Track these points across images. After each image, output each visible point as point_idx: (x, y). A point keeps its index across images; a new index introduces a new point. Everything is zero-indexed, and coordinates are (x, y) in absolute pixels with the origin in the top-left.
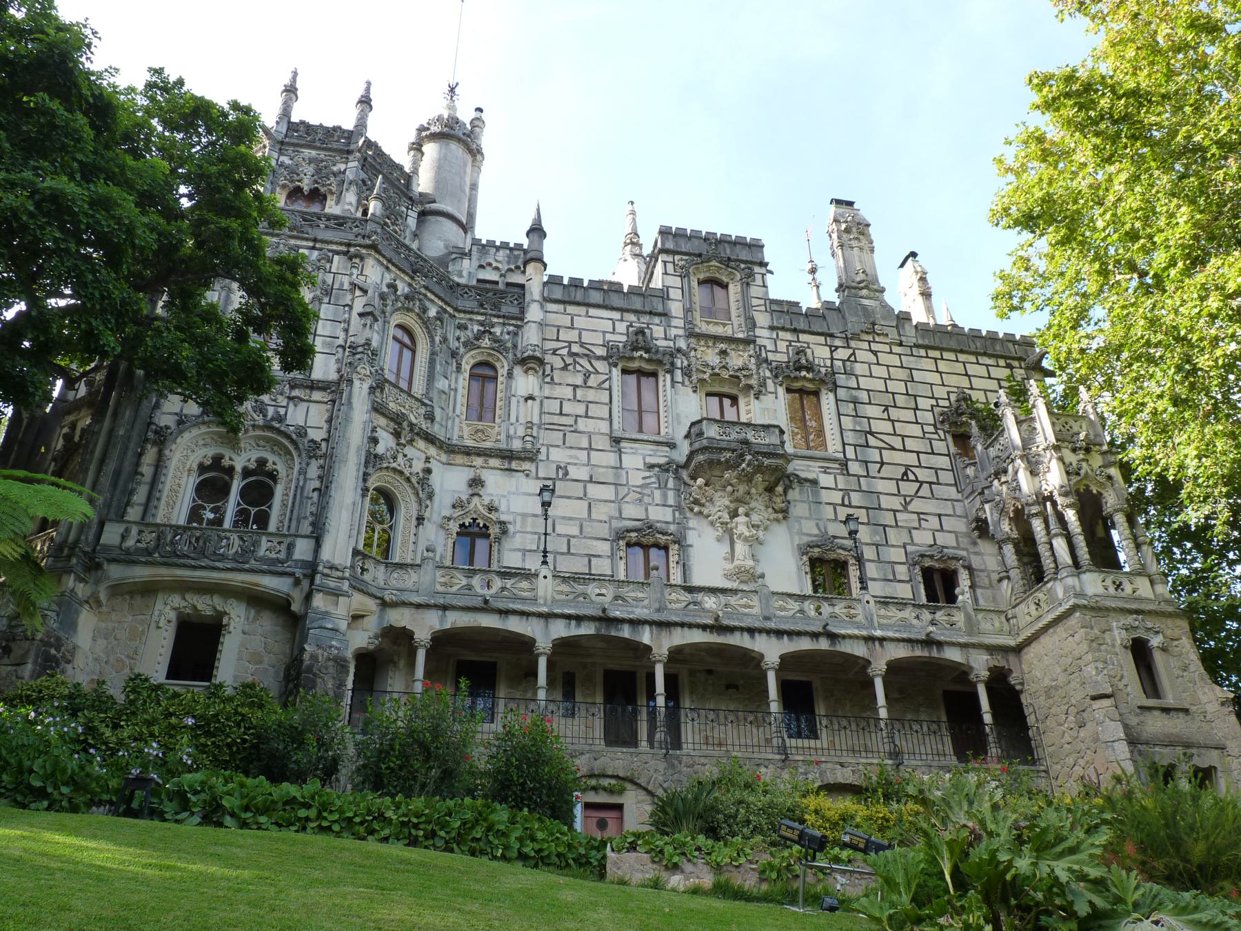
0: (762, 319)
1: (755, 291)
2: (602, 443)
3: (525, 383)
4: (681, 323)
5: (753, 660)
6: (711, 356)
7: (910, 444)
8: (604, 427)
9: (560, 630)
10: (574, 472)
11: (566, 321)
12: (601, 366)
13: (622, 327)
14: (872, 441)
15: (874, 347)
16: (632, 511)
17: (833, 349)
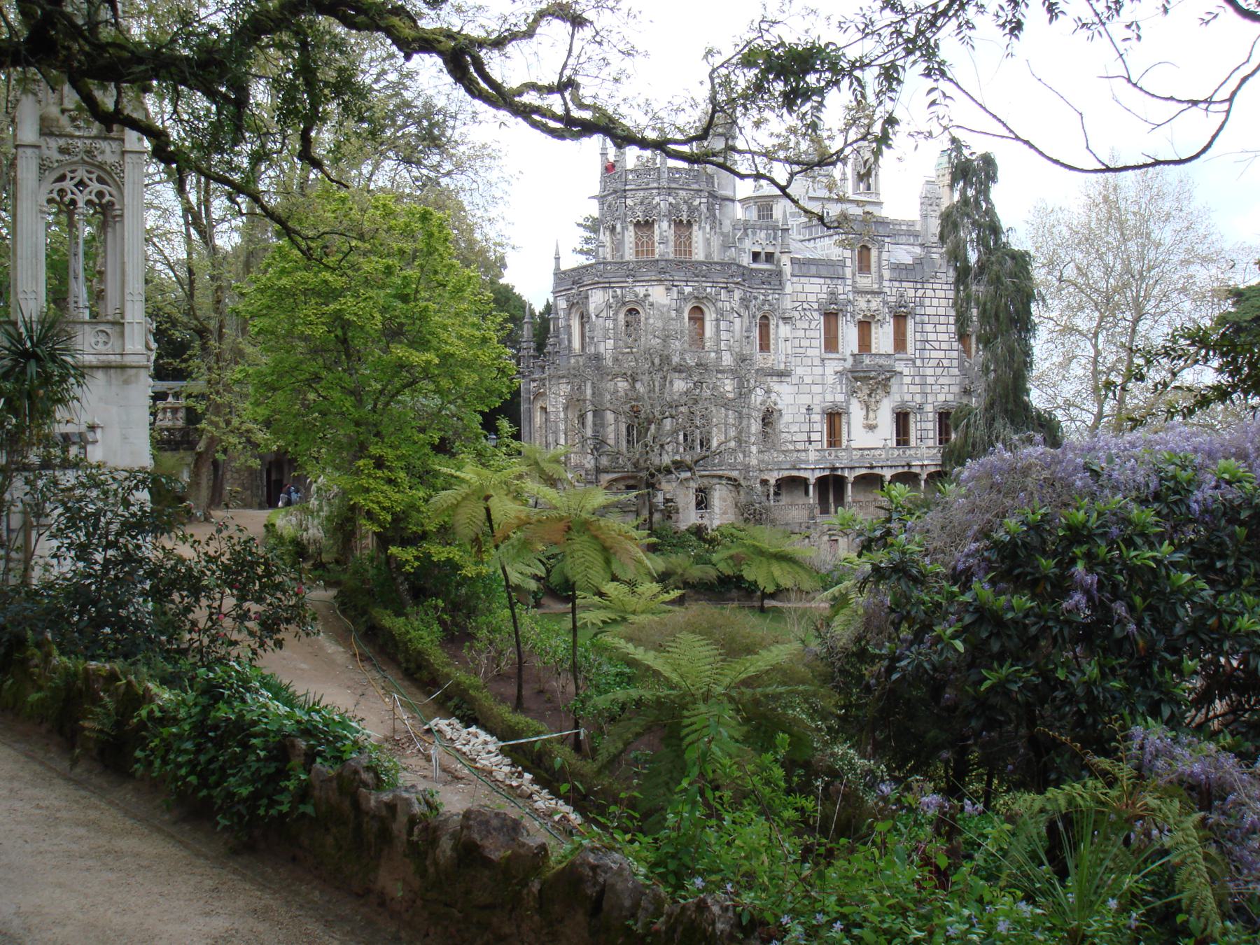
0: (887, 274)
1: (885, 256)
2: (817, 362)
3: (784, 330)
4: (849, 282)
5: (881, 477)
6: (862, 303)
7: (944, 346)
8: (816, 352)
9: (818, 474)
10: (808, 380)
11: (799, 287)
12: (816, 315)
13: (824, 288)
14: (928, 346)
15: (936, 286)
16: (829, 398)
17: (916, 290)
